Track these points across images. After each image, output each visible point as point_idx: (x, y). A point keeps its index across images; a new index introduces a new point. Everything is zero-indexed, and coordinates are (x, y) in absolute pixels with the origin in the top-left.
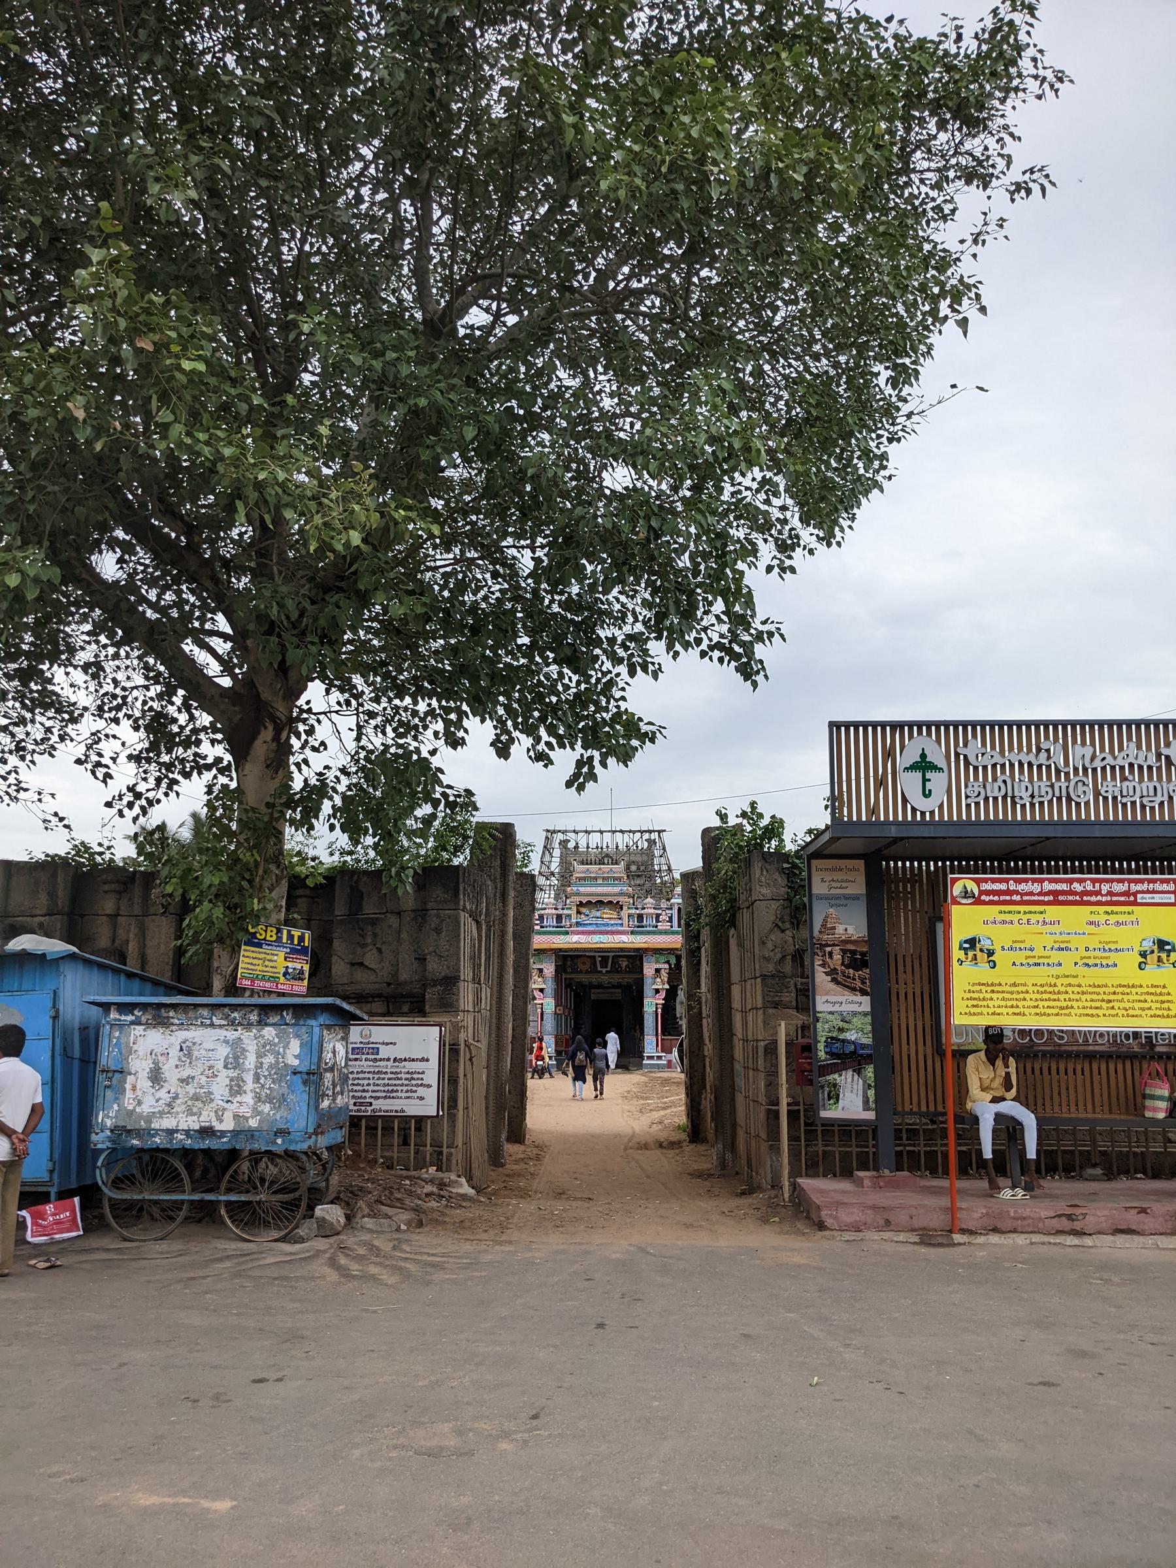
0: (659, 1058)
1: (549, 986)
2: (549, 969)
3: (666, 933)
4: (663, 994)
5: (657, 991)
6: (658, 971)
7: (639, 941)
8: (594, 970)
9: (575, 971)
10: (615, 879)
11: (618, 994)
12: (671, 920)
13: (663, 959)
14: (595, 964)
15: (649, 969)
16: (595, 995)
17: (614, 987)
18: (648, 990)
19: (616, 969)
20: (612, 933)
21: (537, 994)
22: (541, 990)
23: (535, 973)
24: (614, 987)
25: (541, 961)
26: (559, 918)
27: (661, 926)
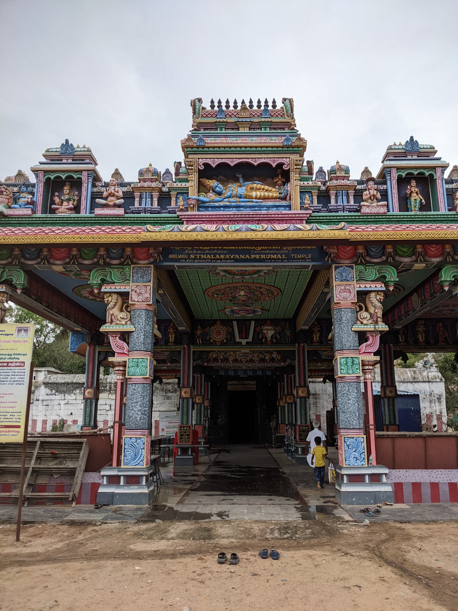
0: (376, 478)
1: (142, 328)
2: (142, 292)
3: (376, 219)
4: (374, 343)
5: (362, 337)
6: (363, 296)
7: (326, 232)
8: (230, 340)
9: (206, 342)
10: (273, 126)
11: (252, 386)
12: (384, 195)
13: (372, 273)
14: (232, 334)
15: (343, 292)
16: (231, 386)
17: (250, 378)
18: (344, 332)
19: (259, 340)
20: (271, 220)
21: (115, 343)
22: (125, 336)
23: (112, 300)
24: (250, 378)
25: (125, 280)
26: (164, 198)
27: (371, 208)
